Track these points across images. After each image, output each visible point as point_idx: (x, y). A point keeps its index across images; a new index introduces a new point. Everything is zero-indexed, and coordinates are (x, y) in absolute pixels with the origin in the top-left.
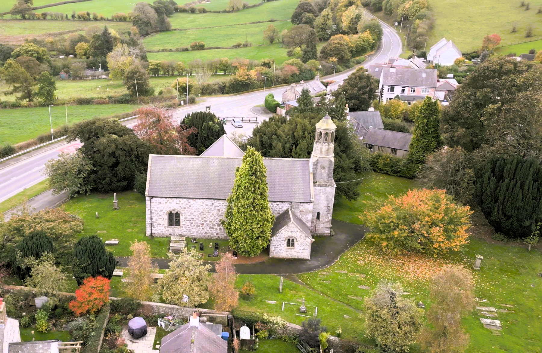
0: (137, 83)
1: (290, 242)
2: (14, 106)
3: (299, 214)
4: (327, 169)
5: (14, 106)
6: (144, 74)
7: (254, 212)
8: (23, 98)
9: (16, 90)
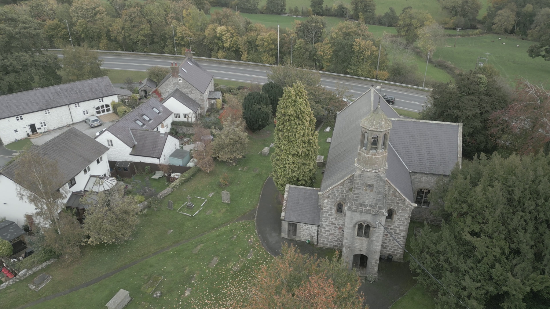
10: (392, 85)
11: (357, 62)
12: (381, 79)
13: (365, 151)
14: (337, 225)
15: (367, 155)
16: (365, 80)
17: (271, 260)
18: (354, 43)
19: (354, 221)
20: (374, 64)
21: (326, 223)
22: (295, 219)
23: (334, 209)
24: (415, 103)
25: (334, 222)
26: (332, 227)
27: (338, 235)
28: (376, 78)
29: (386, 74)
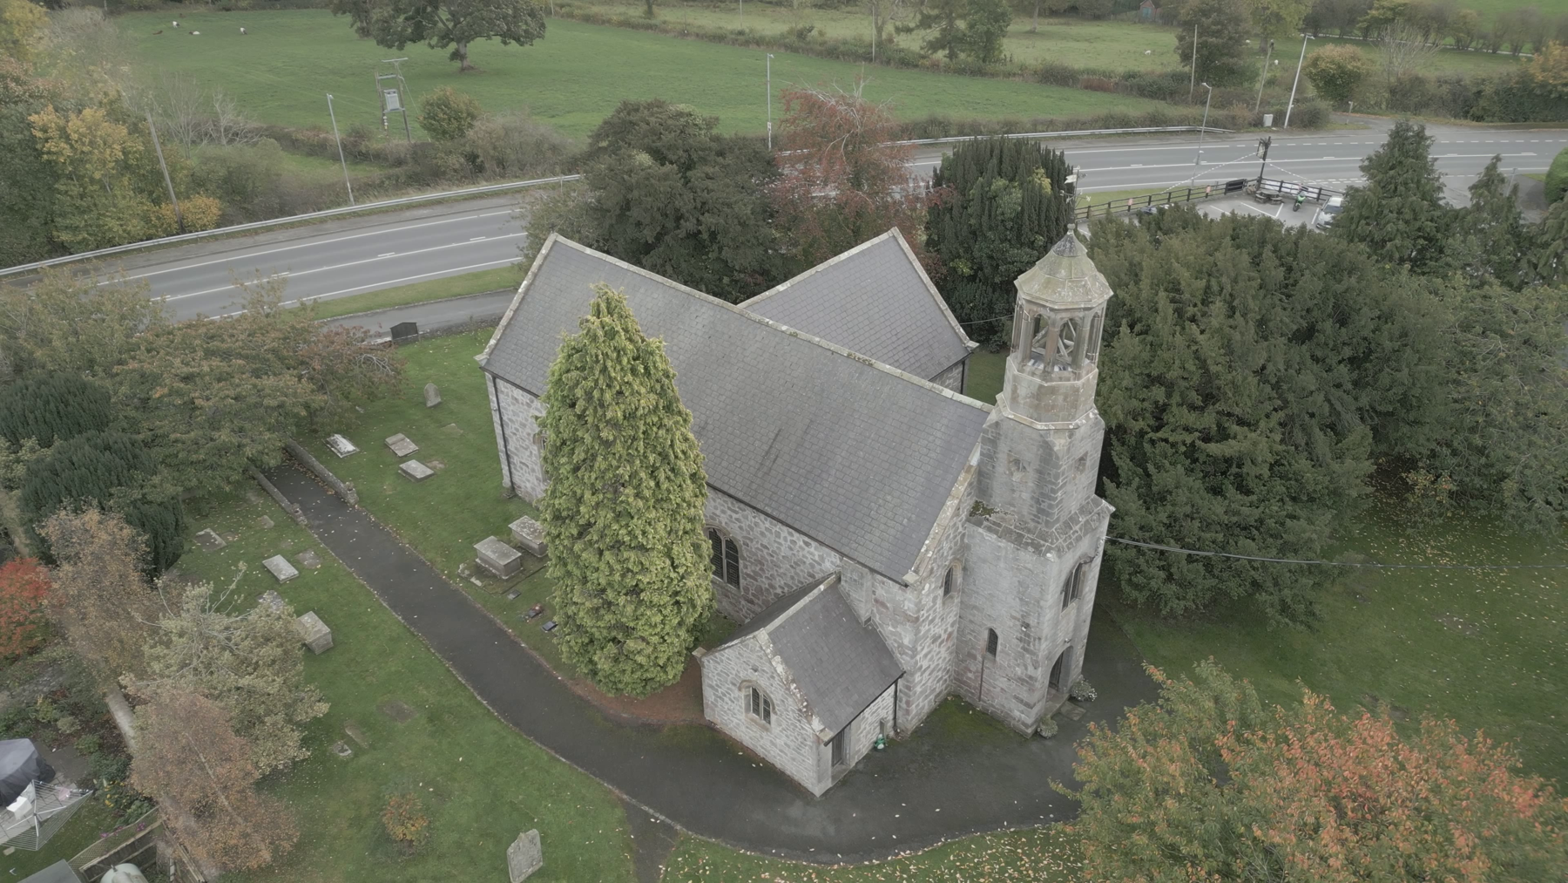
0: (1203, 45)
1: (760, 705)
2: (907, 62)
3: (864, 610)
4: (1031, 475)
5: (907, 62)
6: (1237, 20)
7: (578, 547)
8: (934, 46)
9: (926, 22)
10: (256, 232)
11: (82, 197)
12: (204, 227)
13: (1065, 374)
15: (1079, 383)
16: (149, 249)
17: (905, 870)
18: (39, 134)
20: (150, 184)
22: (850, 710)
23: (941, 592)
24: (388, 256)
28: (183, 230)
29: (207, 205)
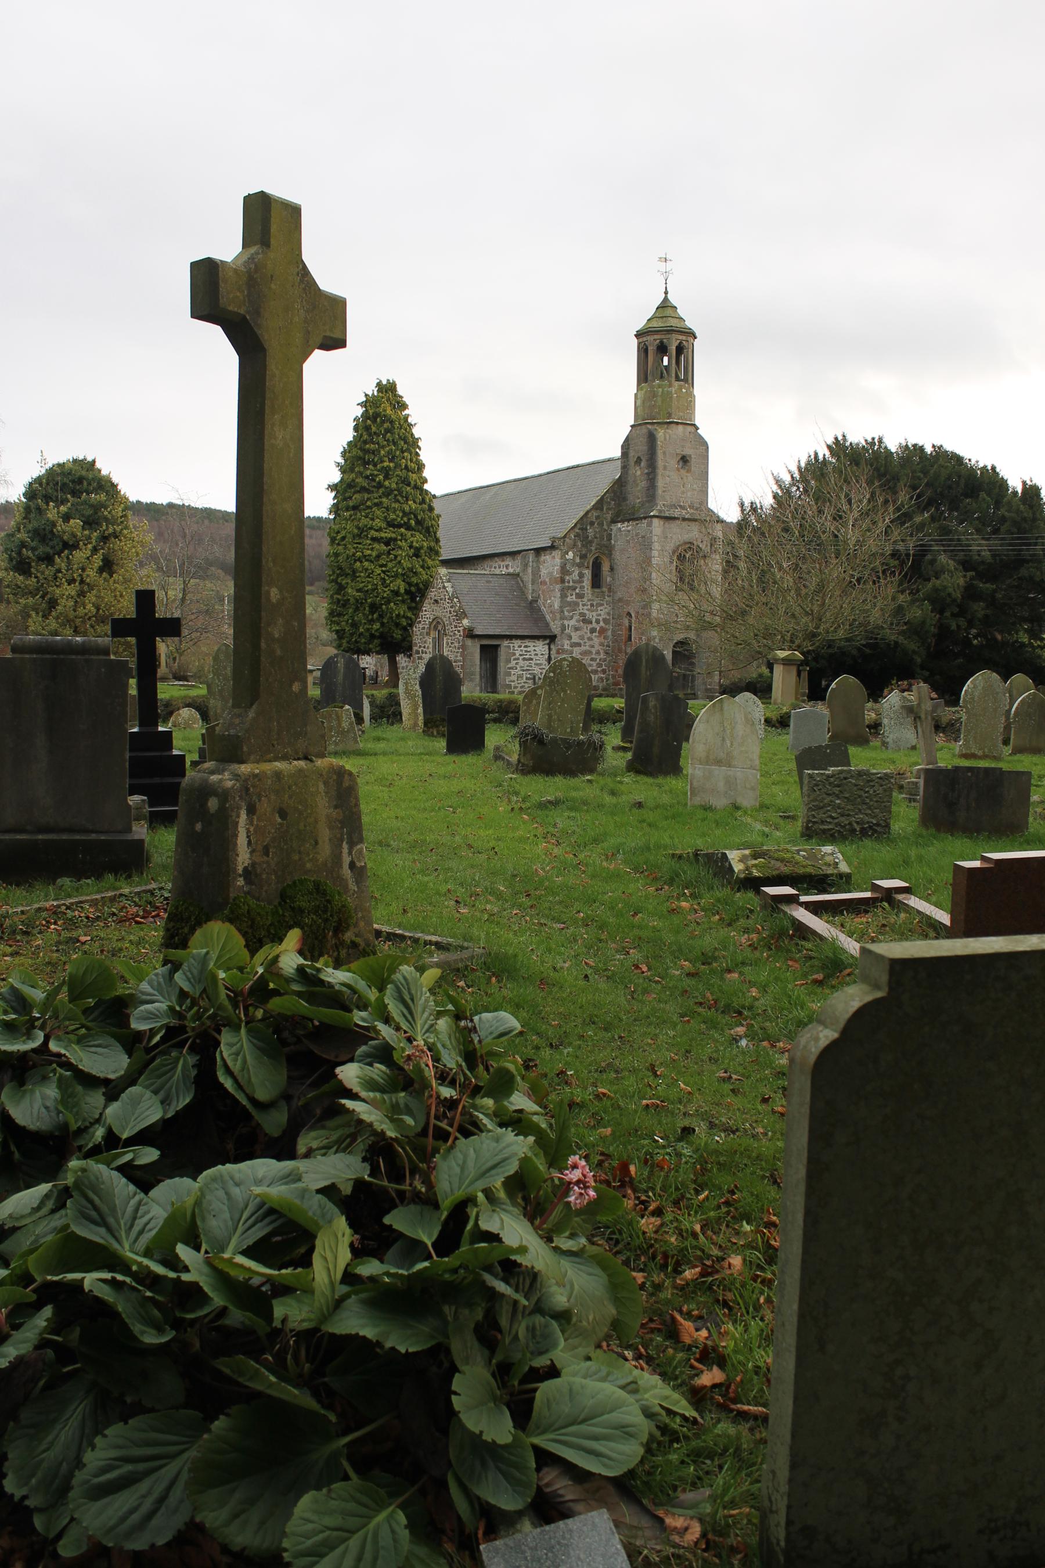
14: (594, 625)
19: (670, 546)
21: (573, 622)
23: (588, 573)
25: (589, 615)
26: (586, 629)
27: (598, 653)
